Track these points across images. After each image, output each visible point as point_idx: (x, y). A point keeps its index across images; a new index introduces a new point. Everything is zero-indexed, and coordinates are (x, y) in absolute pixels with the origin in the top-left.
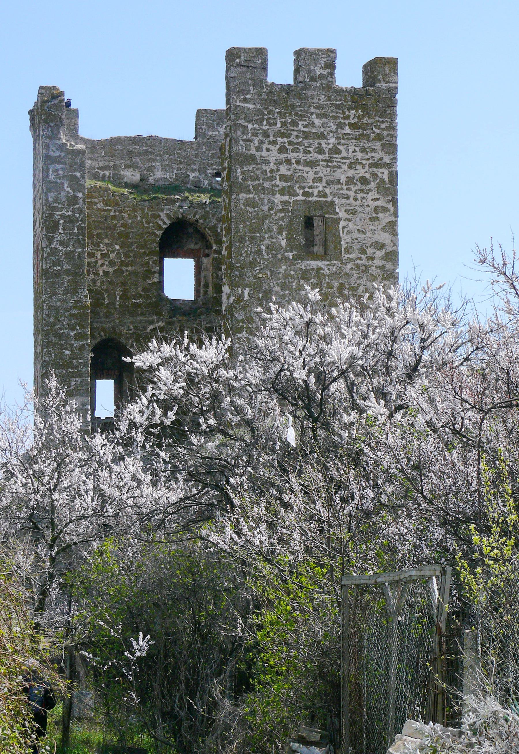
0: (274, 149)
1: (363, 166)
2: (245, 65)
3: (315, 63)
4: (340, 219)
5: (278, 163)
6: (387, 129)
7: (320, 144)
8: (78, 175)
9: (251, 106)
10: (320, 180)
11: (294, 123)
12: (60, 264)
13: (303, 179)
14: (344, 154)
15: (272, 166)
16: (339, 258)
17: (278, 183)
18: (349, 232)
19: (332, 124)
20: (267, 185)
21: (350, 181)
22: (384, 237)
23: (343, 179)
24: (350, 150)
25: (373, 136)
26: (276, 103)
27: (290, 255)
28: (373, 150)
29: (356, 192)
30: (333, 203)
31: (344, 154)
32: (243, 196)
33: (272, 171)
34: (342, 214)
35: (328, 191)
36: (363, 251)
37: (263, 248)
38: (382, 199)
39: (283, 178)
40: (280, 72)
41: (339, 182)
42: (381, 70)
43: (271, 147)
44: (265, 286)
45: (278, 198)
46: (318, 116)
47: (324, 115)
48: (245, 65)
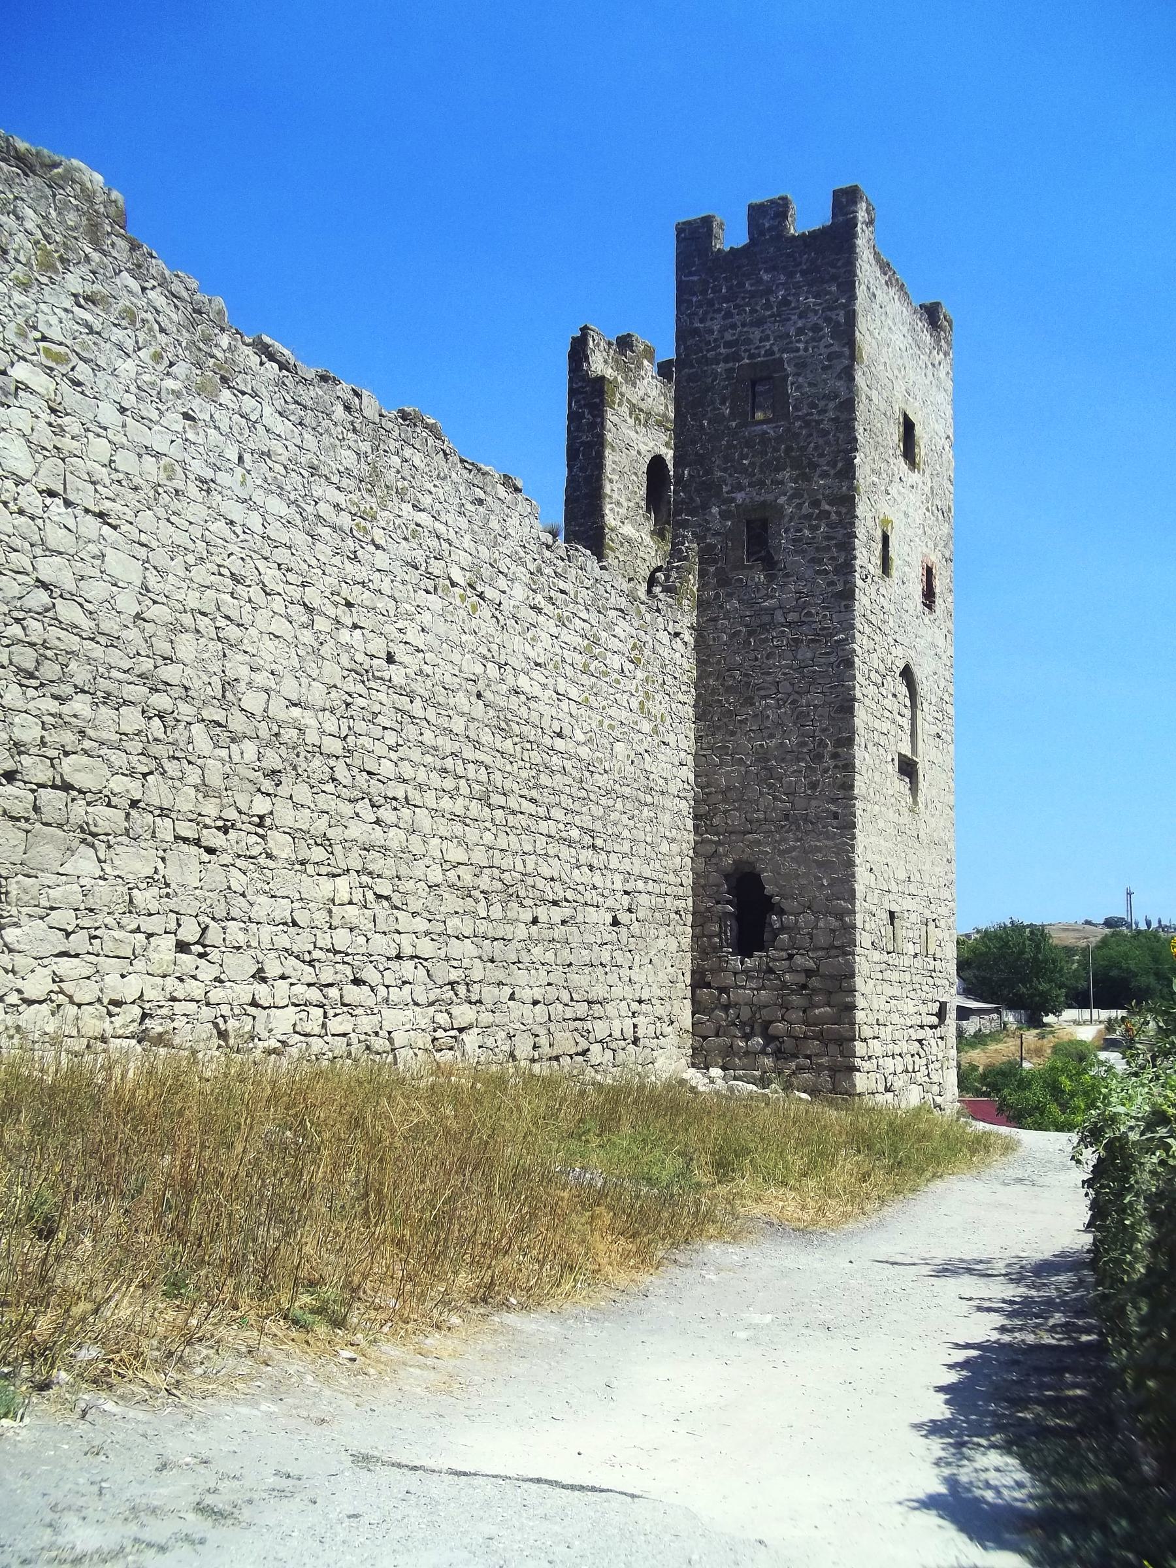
1: (816, 312)
3: (768, 216)
5: (722, 331)
7: (768, 300)
8: (597, 400)
9: (695, 278)
10: (767, 338)
11: (741, 285)
13: (748, 341)
17: (722, 350)
18: (798, 388)
19: (782, 277)
21: (800, 331)
23: (792, 332)
25: (827, 277)
27: (734, 424)
29: (806, 342)
30: (781, 360)
33: (715, 340)
35: (776, 349)
36: (813, 405)
37: (705, 423)
38: (836, 343)
39: (728, 345)
40: (732, 235)
41: (788, 336)
43: (717, 316)
46: (766, 271)
47: (774, 268)
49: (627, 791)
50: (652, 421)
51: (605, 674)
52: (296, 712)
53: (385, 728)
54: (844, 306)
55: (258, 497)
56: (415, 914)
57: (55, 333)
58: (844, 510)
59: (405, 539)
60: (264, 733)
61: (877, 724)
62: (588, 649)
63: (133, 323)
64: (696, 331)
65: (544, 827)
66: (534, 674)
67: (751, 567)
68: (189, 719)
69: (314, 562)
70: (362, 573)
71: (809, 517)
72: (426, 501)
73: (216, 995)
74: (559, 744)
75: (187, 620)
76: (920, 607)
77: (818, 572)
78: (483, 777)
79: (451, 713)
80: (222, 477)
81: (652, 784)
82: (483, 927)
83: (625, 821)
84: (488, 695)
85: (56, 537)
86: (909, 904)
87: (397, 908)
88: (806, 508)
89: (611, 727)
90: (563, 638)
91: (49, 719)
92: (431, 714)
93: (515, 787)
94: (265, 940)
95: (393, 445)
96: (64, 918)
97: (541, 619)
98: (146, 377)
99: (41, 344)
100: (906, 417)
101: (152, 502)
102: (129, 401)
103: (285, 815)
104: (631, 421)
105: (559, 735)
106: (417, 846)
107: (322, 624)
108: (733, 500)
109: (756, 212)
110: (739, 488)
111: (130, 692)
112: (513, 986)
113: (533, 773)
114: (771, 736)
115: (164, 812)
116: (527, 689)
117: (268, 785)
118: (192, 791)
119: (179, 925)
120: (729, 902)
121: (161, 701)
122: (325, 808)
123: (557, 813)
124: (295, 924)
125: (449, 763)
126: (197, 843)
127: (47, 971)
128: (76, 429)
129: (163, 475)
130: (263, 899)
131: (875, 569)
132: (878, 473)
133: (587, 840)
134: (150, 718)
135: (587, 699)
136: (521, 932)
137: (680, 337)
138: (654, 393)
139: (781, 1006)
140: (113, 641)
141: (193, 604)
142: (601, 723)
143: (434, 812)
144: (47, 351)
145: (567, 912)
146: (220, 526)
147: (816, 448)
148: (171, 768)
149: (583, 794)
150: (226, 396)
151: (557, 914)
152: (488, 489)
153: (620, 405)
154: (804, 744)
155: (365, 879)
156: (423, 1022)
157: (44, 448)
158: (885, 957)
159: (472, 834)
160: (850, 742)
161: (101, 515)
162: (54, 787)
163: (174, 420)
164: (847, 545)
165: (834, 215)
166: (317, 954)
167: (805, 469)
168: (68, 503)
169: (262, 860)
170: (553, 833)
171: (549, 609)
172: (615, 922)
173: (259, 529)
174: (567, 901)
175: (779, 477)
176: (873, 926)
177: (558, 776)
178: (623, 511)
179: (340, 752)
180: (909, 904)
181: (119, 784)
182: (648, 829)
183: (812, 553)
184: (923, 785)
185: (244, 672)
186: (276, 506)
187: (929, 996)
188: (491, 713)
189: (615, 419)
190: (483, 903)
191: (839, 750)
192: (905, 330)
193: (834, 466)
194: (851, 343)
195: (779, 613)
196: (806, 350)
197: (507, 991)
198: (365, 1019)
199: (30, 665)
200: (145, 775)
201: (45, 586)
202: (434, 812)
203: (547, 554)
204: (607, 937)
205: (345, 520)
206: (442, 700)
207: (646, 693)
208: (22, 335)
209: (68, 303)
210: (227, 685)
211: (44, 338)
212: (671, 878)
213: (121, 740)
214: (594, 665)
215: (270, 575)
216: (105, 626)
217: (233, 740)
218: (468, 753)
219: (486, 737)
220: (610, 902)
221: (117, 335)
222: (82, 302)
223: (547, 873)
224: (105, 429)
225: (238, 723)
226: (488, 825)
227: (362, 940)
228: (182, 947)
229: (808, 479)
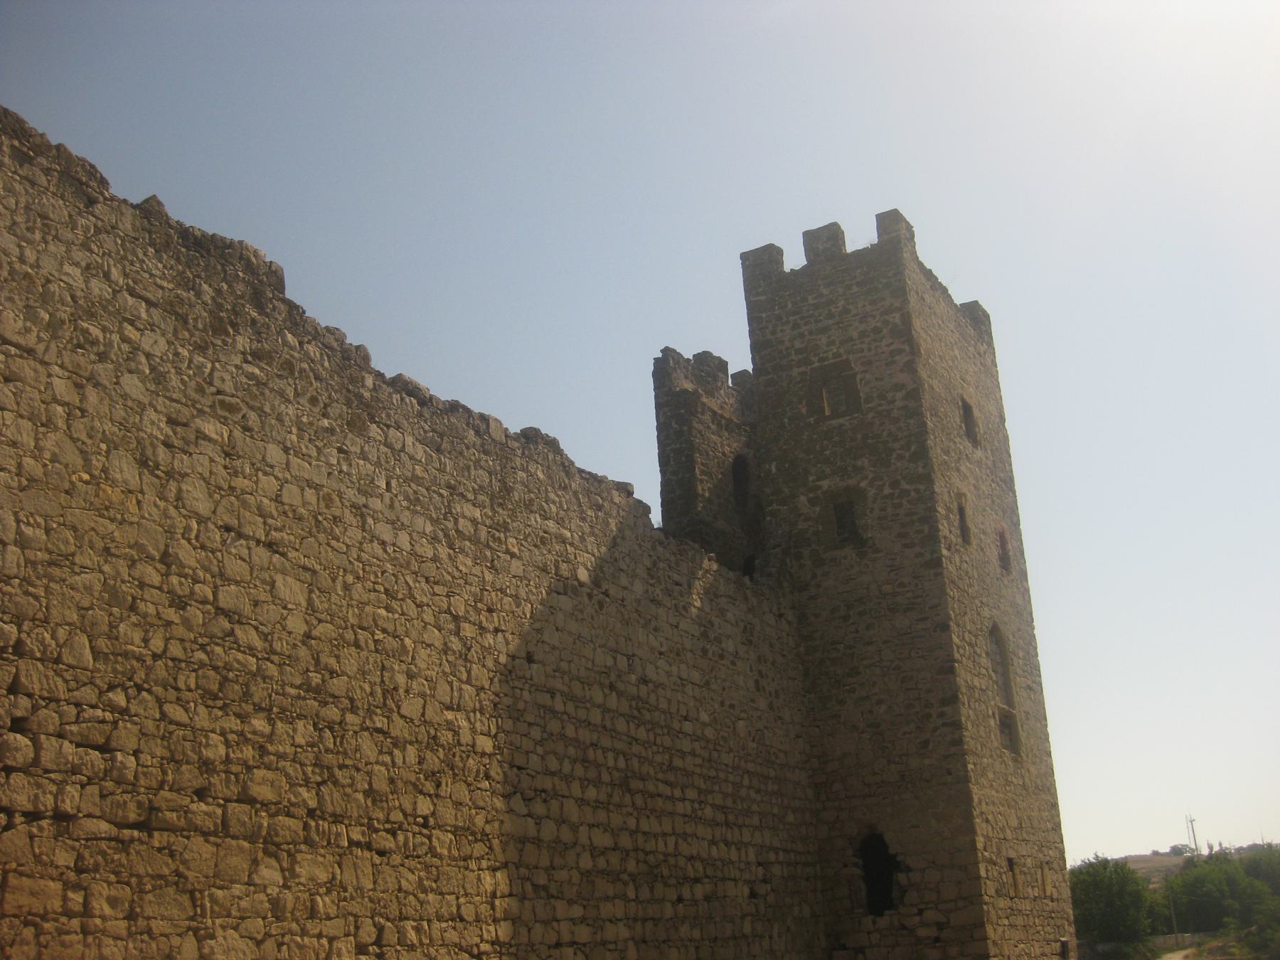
1: (874, 317)
2: (760, 266)
3: (824, 241)
4: (856, 374)
9: (763, 298)
10: (833, 343)
14: (854, 312)
15: (787, 344)
21: (863, 335)
23: (855, 335)
27: (812, 420)
33: (787, 349)
34: (857, 368)
35: (841, 351)
39: (798, 351)
41: (851, 339)
42: (893, 227)
48: (760, 266)
49: (751, 767)
51: (721, 657)
52: (450, 715)
53: (530, 724)
55: (405, 517)
56: (571, 902)
57: (228, 387)
58: (922, 487)
59: (535, 546)
60: (423, 737)
61: (976, 682)
62: (704, 635)
63: (292, 373)
65: (680, 807)
66: (661, 663)
68: (357, 728)
69: (457, 574)
75: (349, 636)
76: (998, 571)
78: (622, 763)
79: (588, 705)
80: (376, 504)
81: (773, 758)
83: (753, 795)
87: (553, 896)
89: (732, 706)
90: (681, 626)
92: (570, 708)
93: (652, 772)
94: (436, 934)
95: (518, 461)
97: (661, 611)
99: (220, 397)
100: (963, 400)
101: (314, 530)
103: (448, 814)
105: (686, 719)
106: (566, 835)
107: (468, 630)
108: (820, 487)
113: (667, 757)
114: (879, 702)
117: (429, 787)
118: (360, 796)
119: (357, 928)
121: (332, 713)
122: (481, 804)
123: (691, 794)
124: (462, 920)
125: (591, 754)
126: (369, 846)
129: (322, 504)
131: (955, 538)
132: (947, 452)
133: (720, 817)
134: (321, 730)
135: (708, 683)
136: (669, 911)
137: (756, 348)
141: (353, 620)
142: (722, 704)
143: (581, 802)
144: (222, 403)
145: (708, 888)
149: (712, 773)
150: (374, 430)
151: (699, 891)
152: (605, 495)
153: (703, 413)
155: (523, 871)
157: (221, 489)
158: (1008, 903)
159: (616, 819)
160: (953, 700)
162: (237, 801)
164: (930, 518)
169: (428, 858)
170: (689, 812)
172: (753, 895)
174: (707, 877)
175: (859, 463)
176: (995, 874)
177: (689, 759)
180: (1024, 850)
182: (774, 801)
185: (401, 679)
187: (1052, 937)
190: (631, 886)
191: (945, 709)
192: (952, 327)
196: (870, 350)
199: (215, 687)
200: (319, 784)
201: (226, 613)
202: (581, 802)
203: (660, 549)
207: (760, 672)
209: (237, 360)
211: (219, 392)
213: (296, 752)
214: (712, 649)
217: (395, 745)
218: (606, 742)
219: (621, 725)
220: (747, 876)
222: (250, 358)
223: (685, 849)
224: (272, 467)
225: (399, 728)
226: (630, 810)
227: (524, 931)
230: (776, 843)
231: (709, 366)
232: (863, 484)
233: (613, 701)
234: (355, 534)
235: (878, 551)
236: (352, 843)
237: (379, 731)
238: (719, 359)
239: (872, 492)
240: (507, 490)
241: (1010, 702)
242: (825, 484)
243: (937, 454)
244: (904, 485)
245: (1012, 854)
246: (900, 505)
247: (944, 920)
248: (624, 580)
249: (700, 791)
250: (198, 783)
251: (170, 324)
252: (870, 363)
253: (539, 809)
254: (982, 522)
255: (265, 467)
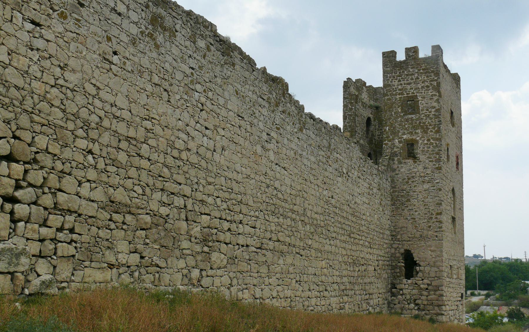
0: (397, 81)
1: (427, 82)
3: (412, 52)
5: (398, 85)
6: (436, 68)
11: (403, 72)
12: (347, 129)
14: (420, 79)
16: (419, 113)
18: (422, 104)
20: (394, 93)
21: (423, 87)
22: (435, 104)
23: (420, 87)
24: (423, 77)
26: (397, 67)
28: (431, 76)
31: (420, 79)
32: (386, 97)
34: (420, 98)
39: (400, 90)
44: (394, 126)
45: (398, 97)
46: (411, 68)
48: (389, 57)
49: (377, 229)
50: (367, 107)
54: (436, 80)
57: (278, 123)
58: (438, 142)
60: (311, 222)
62: (369, 187)
64: (389, 85)
67: (409, 159)
69: (319, 173)
70: (327, 174)
71: (427, 144)
72: (339, 150)
73: (303, 295)
74: (364, 217)
77: (430, 161)
80: (304, 153)
82: (350, 273)
84: (350, 205)
85: (278, 175)
86: (454, 263)
88: (426, 142)
91: (276, 224)
96: (278, 275)
98: (292, 130)
102: (289, 137)
104: (362, 107)
108: (403, 137)
109: (408, 50)
110: (404, 134)
111: (290, 214)
112: (354, 290)
114: (416, 211)
115: (294, 246)
116: (358, 202)
120: (402, 262)
121: (294, 216)
123: (363, 238)
124: (315, 274)
127: (276, 290)
128: (280, 147)
130: (310, 268)
131: (446, 160)
132: (445, 130)
138: (366, 97)
139: (420, 295)
140: (285, 201)
141: (299, 189)
145: (365, 267)
146: (303, 166)
147: (429, 123)
148: (295, 233)
151: (364, 268)
154: (426, 214)
156: (338, 301)
159: (347, 246)
161: (284, 168)
163: (296, 140)
165: (432, 53)
166: (320, 283)
167: (425, 131)
168: (279, 166)
169: (310, 258)
171: (362, 177)
172: (375, 270)
173: (309, 166)
175: (417, 131)
178: (360, 136)
179: (323, 225)
180: (454, 263)
181: (288, 240)
183: (428, 155)
184: (457, 225)
186: (313, 159)
188: (351, 210)
189: (358, 107)
193: (434, 129)
194: (439, 92)
195: (418, 173)
197: (353, 291)
198: (328, 301)
199: (273, 210)
204: (374, 274)
205: (324, 160)
206: (342, 208)
208: (273, 124)
209: (280, 114)
210: (304, 209)
211: (276, 124)
212: (386, 255)
214: (371, 192)
215: (312, 177)
216: (285, 198)
218: (347, 223)
220: (374, 264)
221: (287, 120)
223: (362, 256)
225: (306, 220)
228: (297, 281)
229: (427, 133)
230: (381, 254)
231: (360, 84)
232: (418, 138)
233: (348, 210)
234: (299, 164)
235: (420, 162)
236: (297, 253)
237: (303, 221)
238: (364, 82)
239: (420, 142)
240: (330, 145)
241: (454, 214)
242: (405, 137)
243: (443, 132)
244: (432, 141)
245: (452, 264)
246: (429, 147)
247: (430, 283)
248: (353, 171)
249: (366, 237)
250: (270, 237)
251: (267, 105)
252: (424, 98)
253: (332, 242)
254: (453, 153)
255: (283, 145)
